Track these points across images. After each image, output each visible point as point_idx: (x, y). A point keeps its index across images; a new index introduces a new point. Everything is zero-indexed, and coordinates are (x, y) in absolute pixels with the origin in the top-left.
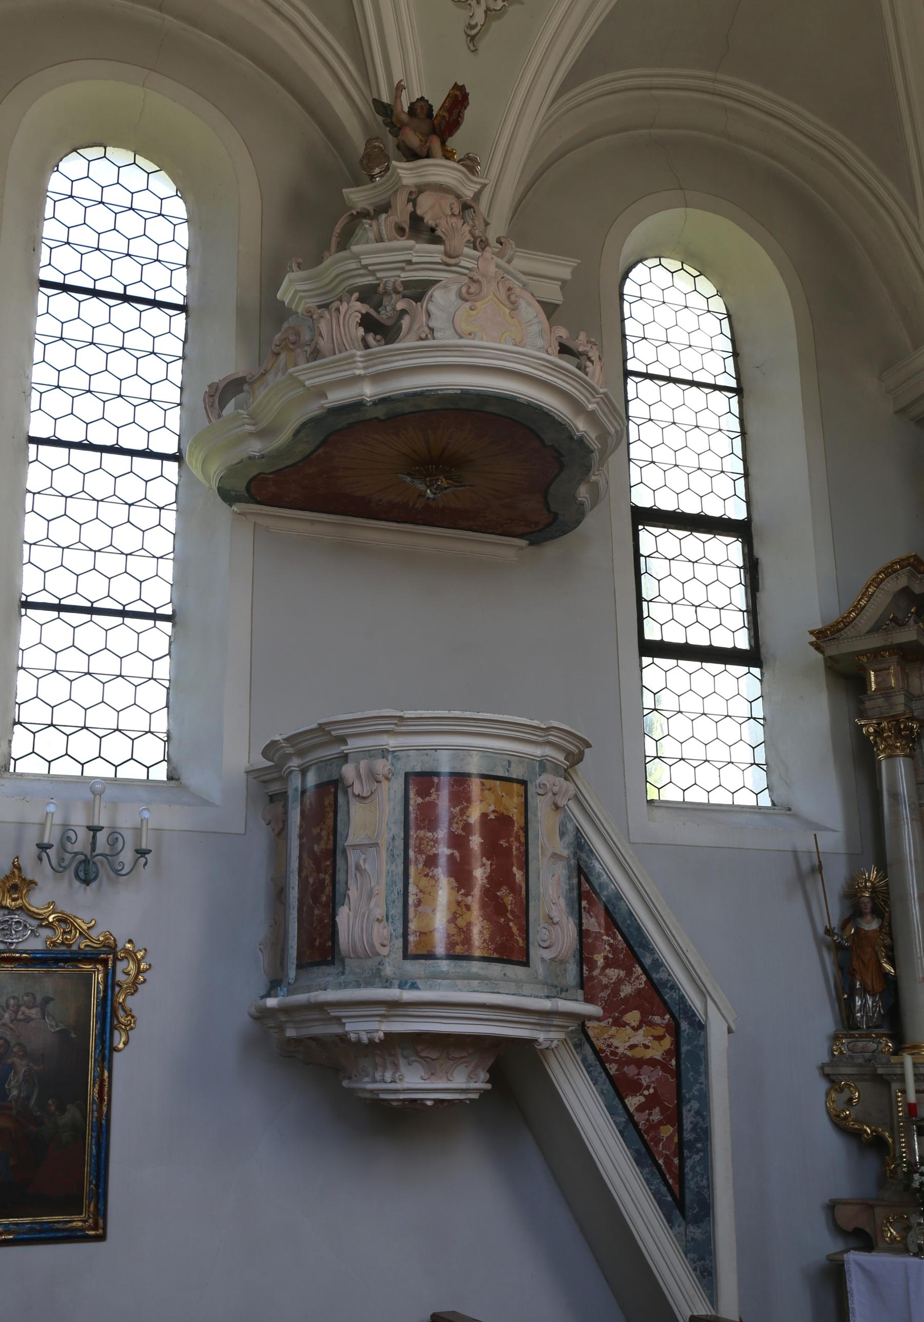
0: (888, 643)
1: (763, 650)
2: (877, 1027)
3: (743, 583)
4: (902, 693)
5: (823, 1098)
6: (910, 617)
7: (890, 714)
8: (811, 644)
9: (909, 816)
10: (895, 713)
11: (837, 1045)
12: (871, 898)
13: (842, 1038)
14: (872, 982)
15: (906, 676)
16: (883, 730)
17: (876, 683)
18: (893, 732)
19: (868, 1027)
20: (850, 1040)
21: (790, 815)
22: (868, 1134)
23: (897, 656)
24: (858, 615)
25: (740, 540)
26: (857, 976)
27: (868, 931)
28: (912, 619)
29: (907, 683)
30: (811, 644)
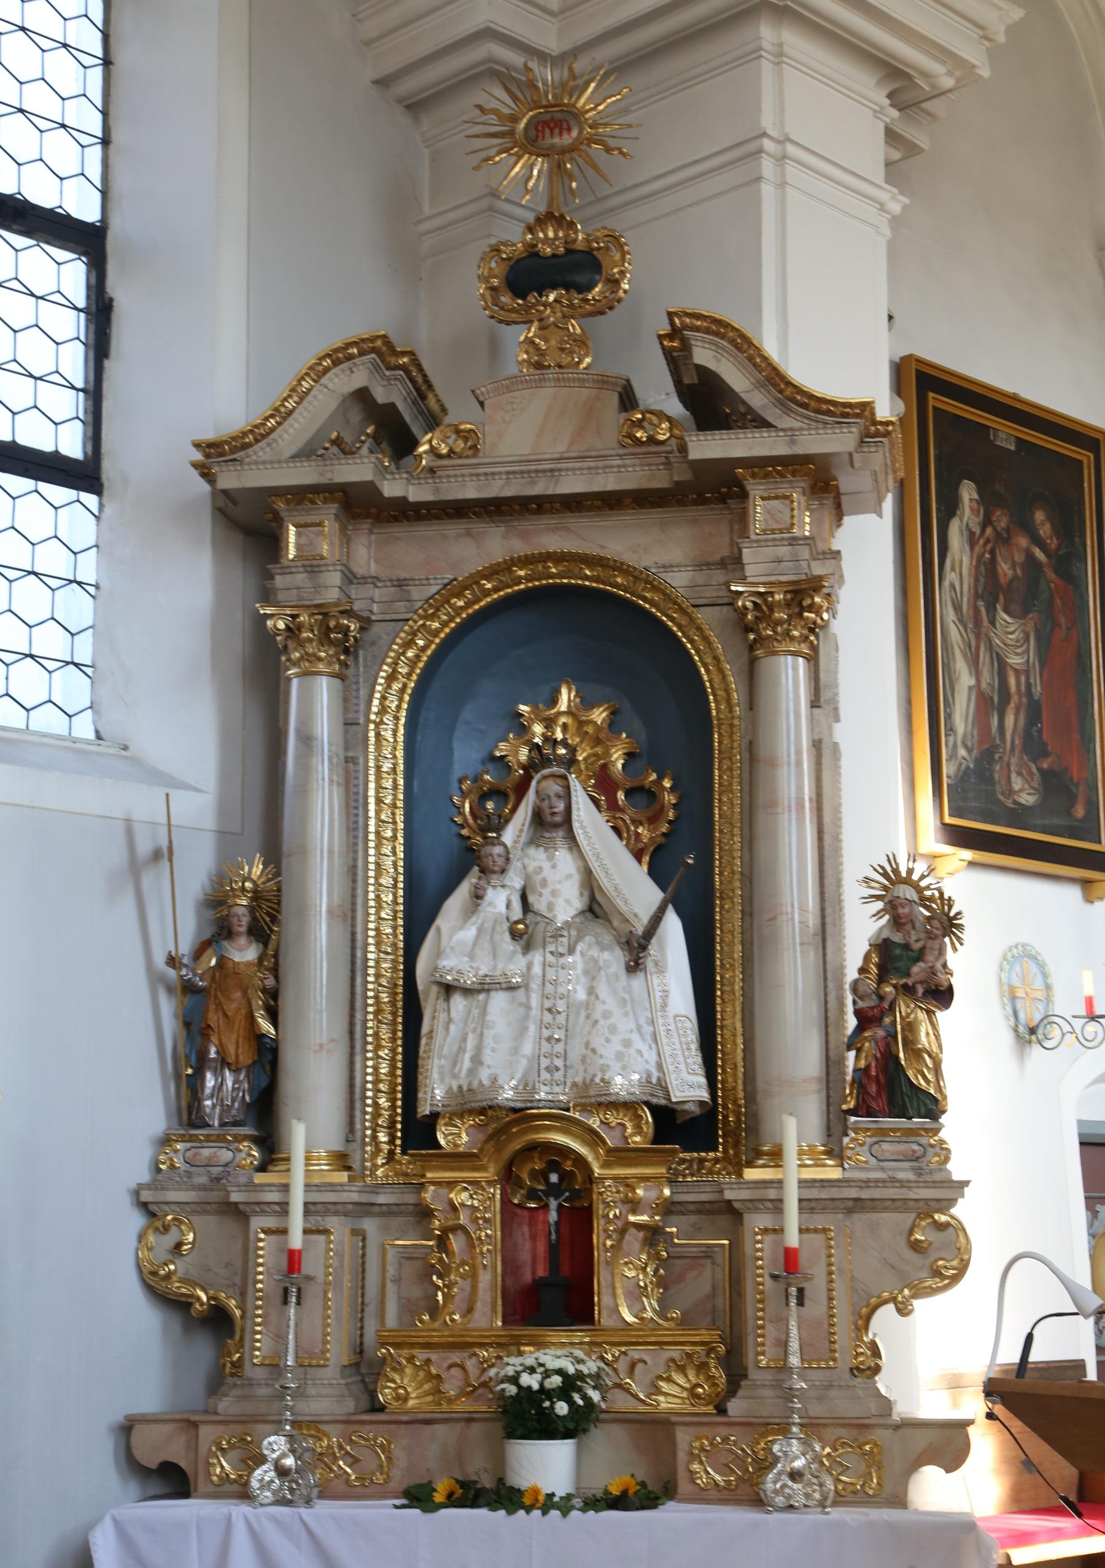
0: (324, 480)
2: (236, 1124)
3: (82, 338)
4: (339, 568)
5: (133, 1243)
6: (363, 442)
8: (195, 465)
9: (326, 777)
12: (252, 909)
13: (177, 1141)
15: (347, 540)
16: (300, 628)
17: (298, 546)
19: (223, 1124)
20: (189, 1145)
22: (202, 1304)
23: (336, 505)
24: (279, 424)
25: (84, 259)
27: (238, 963)
30: (195, 465)
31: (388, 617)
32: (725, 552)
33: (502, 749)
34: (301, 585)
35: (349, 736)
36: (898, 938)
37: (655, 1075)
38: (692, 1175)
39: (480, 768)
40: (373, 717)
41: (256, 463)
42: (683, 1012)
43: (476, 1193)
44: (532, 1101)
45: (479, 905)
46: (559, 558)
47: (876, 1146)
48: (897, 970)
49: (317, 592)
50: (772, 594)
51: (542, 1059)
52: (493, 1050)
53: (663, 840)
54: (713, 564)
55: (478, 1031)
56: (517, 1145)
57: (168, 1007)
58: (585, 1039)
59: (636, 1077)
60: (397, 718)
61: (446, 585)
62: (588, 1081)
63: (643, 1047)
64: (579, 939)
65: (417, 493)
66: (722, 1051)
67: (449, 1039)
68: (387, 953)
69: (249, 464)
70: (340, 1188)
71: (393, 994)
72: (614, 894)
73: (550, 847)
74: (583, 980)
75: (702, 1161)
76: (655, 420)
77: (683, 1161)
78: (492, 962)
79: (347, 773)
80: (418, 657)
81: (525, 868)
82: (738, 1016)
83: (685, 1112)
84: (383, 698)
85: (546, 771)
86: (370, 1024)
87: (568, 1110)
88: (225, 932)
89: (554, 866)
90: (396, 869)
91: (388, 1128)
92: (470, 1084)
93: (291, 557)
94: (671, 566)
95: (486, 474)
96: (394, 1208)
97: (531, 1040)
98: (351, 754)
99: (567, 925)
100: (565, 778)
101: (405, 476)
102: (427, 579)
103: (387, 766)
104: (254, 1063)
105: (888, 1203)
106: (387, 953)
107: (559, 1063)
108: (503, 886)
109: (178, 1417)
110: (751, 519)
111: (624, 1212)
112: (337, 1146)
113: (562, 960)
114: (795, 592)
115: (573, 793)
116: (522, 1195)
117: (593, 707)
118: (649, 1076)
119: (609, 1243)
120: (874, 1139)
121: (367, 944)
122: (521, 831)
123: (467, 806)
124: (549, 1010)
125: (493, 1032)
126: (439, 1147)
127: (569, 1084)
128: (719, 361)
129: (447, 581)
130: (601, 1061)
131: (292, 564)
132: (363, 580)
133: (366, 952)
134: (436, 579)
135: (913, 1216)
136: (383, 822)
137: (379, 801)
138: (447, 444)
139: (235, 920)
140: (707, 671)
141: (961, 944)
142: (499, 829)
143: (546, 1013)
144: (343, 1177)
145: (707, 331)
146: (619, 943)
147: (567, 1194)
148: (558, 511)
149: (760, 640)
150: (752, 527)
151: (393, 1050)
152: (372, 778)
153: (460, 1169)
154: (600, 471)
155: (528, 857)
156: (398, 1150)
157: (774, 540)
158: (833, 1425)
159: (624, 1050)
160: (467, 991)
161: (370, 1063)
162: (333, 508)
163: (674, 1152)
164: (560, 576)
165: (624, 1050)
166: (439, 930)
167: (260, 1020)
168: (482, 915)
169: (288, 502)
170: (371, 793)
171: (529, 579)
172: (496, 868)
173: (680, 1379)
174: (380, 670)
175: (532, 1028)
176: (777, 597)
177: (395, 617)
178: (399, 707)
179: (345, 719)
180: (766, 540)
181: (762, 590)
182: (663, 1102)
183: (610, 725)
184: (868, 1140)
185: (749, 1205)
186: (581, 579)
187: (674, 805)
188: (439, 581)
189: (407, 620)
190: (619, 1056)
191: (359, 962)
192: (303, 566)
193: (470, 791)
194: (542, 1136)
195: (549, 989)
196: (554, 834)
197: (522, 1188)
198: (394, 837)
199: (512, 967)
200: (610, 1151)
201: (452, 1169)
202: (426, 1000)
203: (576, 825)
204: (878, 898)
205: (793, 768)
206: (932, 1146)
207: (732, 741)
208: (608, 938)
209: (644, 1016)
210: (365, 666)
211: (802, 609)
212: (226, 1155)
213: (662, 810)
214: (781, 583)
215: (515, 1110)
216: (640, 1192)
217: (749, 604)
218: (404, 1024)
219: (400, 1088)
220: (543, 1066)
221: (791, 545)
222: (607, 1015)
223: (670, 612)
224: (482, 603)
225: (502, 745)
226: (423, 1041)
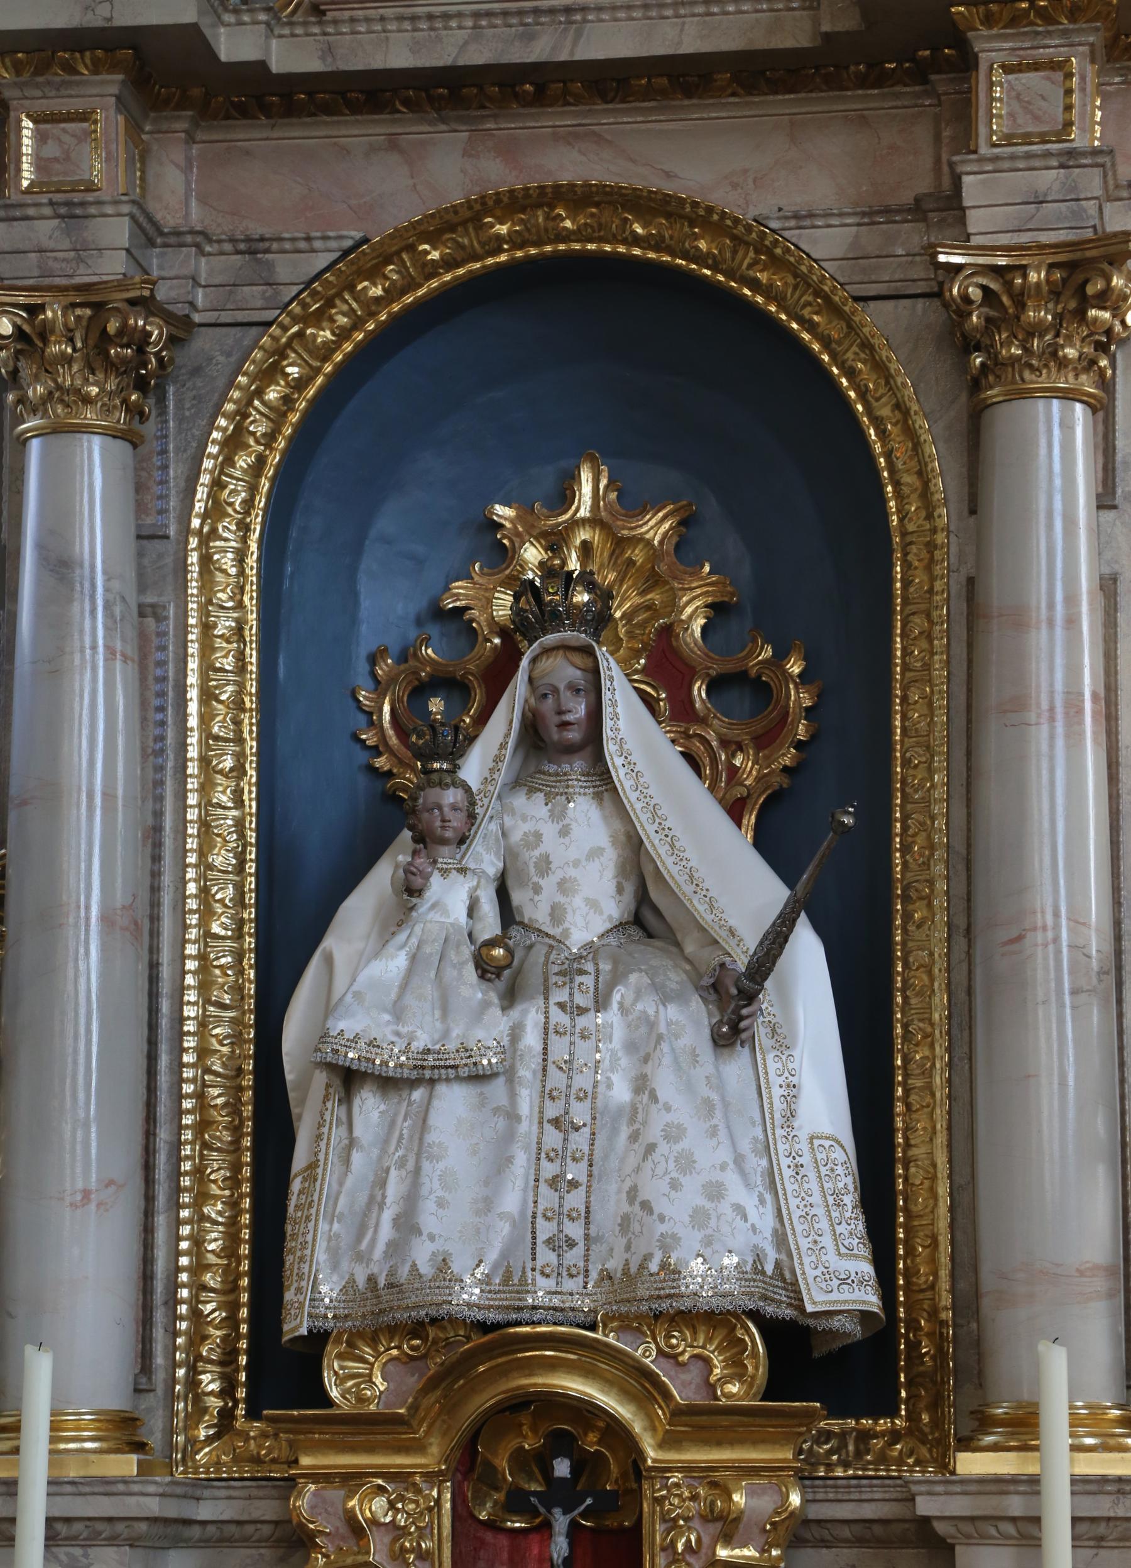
0: (95, 20)
4: (126, 209)
7: (77, 280)
9: (101, 642)
10: (95, 279)
15: (141, 156)
16: (45, 333)
17: (40, 164)
18: (79, 345)
23: (120, 77)
29: (142, 179)
31: (226, 317)
32: (923, 185)
33: (460, 593)
34: (51, 244)
35: (146, 561)
37: (771, 1256)
38: (846, 1465)
39: (413, 633)
40: (196, 523)
42: (828, 1130)
43: (402, 1498)
44: (519, 1309)
45: (412, 908)
49: (80, 260)
50: (1023, 270)
51: (540, 1220)
52: (441, 1204)
53: (785, 782)
54: (898, 212)
55: (411, 1165)
56: (486, 1399)
58: (628, 1184)
59: (733, 1260)
60: (244, 528)
61: (346, 253)
62: (633, 1269)
63: (750, 1203)
64: (617, 978)
66: (906, 1210)
67: (350, 1181)
70: (121, 1487)
72: (689, 889)
74: (624, 1062)
75: (864, 1436)
77: (827, 1435)
78: (438, 1024)
79: (143, 637)
80: (287, 400)
81: (504, 834)
82: (941, 1139)
83: (832, 1333)
84: (218, 484)
85: (551, 638)
86: (187, 1151)
87: (593, 1327)
89: (564, 832)
90: (242, 835)
91: (221, 1363)
92: (392, 1273)
93: (25, 183)
94: (811, 215)
96: (233, 1528)
97: (519, 1183)
98: (150, 599)
99: (591, 950)
100: (588, 651)
101: (262, 17)
102: (308, 239)
103: (224, 625)
107: (574, 1230)
108: (463, 871)
110: (982, 112)
111: (706, 1540)
112: (116, 1400)
113: (582, 1022)
114: (1071, 267)
115: (605, 684)
116: (496, 1503)
117: (644, 512)
118: (759, 1259)
121: (182, 989)
122: (498, 759)
123: (387, 708)
124: (556, 1122)
125: (441, 1166)
126: (328, 1402)
127: (594, 1275)
129: (348, 243)
130: (662, 1228)
131: (29, 199)
132: (176, 238)
133: (179, 1004)
134: (325, 238)
136: (217, 738)
137: (208, 696)
140: (882, 434)
142: (456, 752)
143: (549, 1128)
144: (128, 1464)
147: (589, 1501)
148: (578, 100)
149: (996, 366)
150: (982, 130)
151: (233, 1204)
152: (193, 648)
153: (370, 1449)
154: (669, 12)
155: (513, 812)
156: (241, 1411)
157: (1029, 156)
159: (708, 1205)
160: (388, 1084)
161: (185, 1230)
162: (112, 83)
163: (809, 1416)
164: (577, 235)
165: (708, 1205)
166: (329, 960)
168: (418, 929)
169: (18, 68)
170: (192, 679)
171: (517, 240)
172: (449, 834)
174: (211, 426)
175: (521, 1160)
176: (1033, 277)
177: (241, 316)
178: (249, 504)
179: (139, 527)
180: (1013, 157)
181: (1002, 261)
182: (788, 1313)
183: (678, 547)
185: (968, 1528)
186: (624, 242)
187: (807, 709)
188: (333, 244)
189: (269, 324)
190: (699, 1217)
191: (164, 1023)
193: (392, 680)
194: (539, 1380)
195: (556, 1078)
196: (566, 767)
197: (497, 1489)
198: (239, 770)
199: (480, 1034)
200: (679, 1413)
201: (353, 1449)
202: (302, 1102)
203: (610, 748)
205: (1059, 631)
207: (932, 579)
208: (675, 978)
209: (749, 1135)
210: (180, 420)
211: (1085, 302)
213: (783, 718)
214: (1042, 247)
215: (484, 1327)
216: (739, 1498)
217: (975, 293)
218: (256, 1149)
219: (245, 1282)
220: (541, 1237)
221: (1062, 166)
222: (673, 1134)
223: (806, 312)
224: (420, 292)
225: (460, 587)
226: (296, 1186)
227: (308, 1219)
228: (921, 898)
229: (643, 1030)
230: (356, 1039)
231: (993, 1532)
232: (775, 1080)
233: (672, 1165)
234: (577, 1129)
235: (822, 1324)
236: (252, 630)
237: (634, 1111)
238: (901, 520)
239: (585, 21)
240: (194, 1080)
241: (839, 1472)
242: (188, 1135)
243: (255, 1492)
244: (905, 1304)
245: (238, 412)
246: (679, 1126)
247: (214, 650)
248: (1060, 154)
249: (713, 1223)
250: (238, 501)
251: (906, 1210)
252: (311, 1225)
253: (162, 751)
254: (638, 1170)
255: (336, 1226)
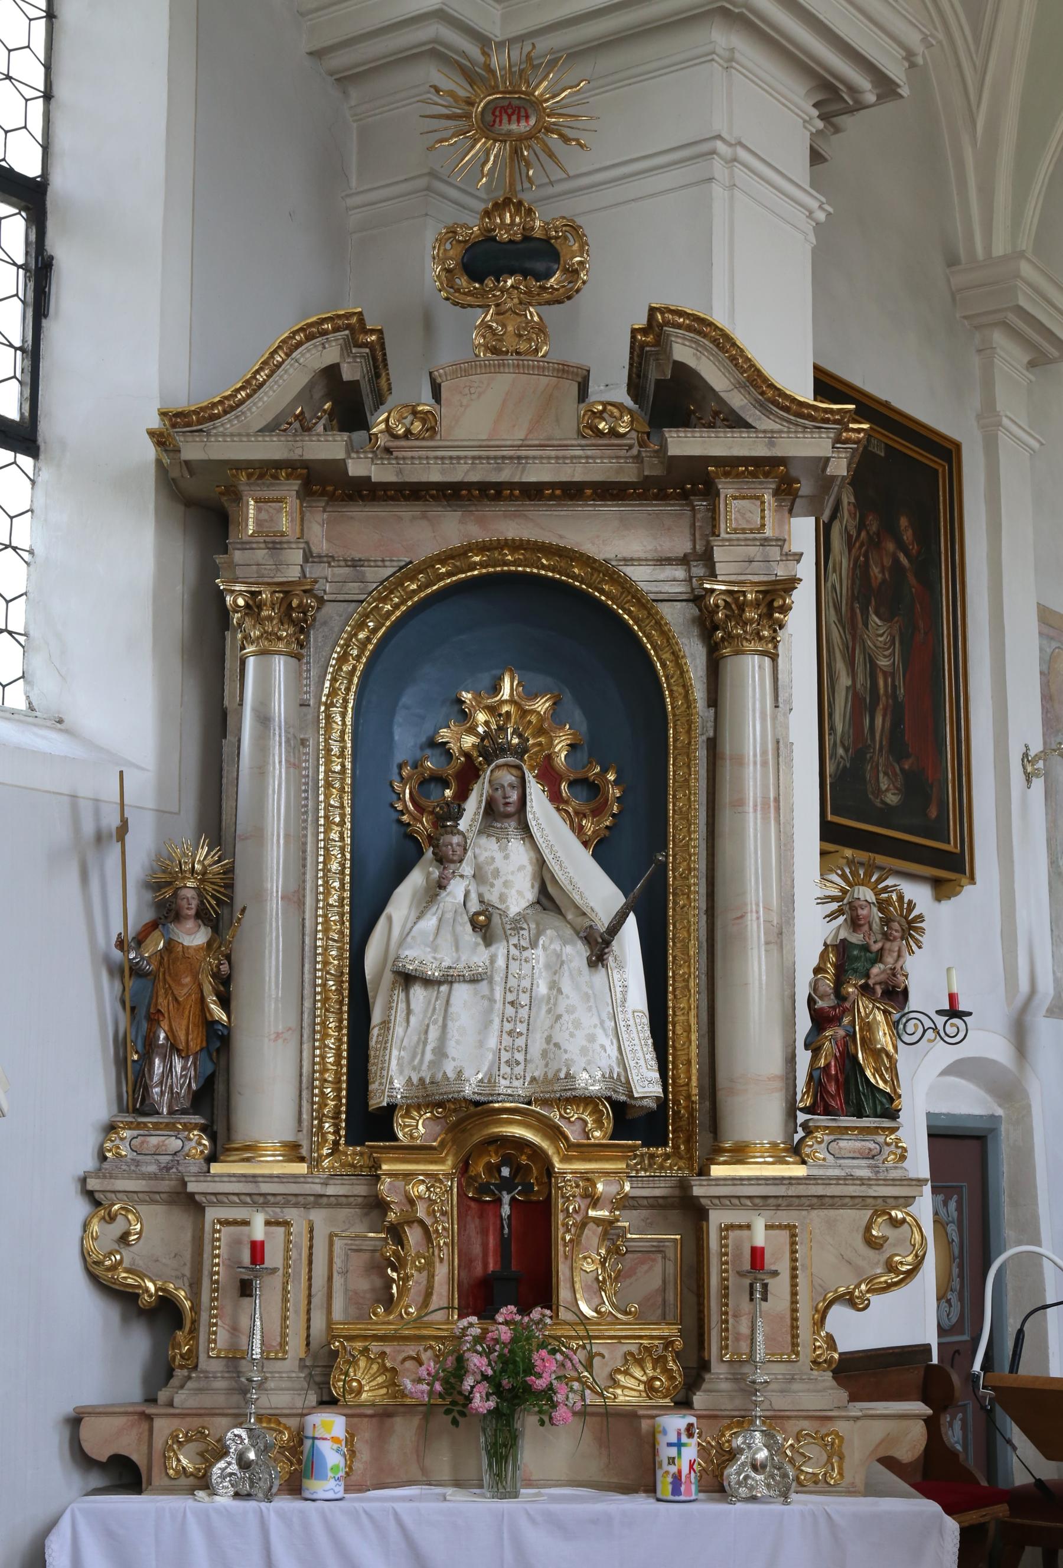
0: (295, 455)
1: (43, 426)
2: (184, 1112)
3: (21, 295)
5: (78, 1232)
6: (320, 418)
7: (276, 580)
8: (151, 433)
11: (112, 1141)
12: (200, 892)
13: (123, 1128)
14: (187, 1034)
16: (260, 606)
17: (258, 522)
19: (171, 1112)
20: (135, 1133)
21: (61, 730)
22: (150, 1296)
23: (299, 482)
24: (249, 396)
25: (23, 214)
26: (162, 1024)
27: (188, 948)
28: (323, 421)
30: (151, 433)
31: (340, 597)
34: (261, 561)
36: (856, 939)
37: (616, 1070)
38: (646, 1171)
40: (324, 699)
41: (224, 435)
43: (433, 1186)
44: (492, 1095)
46: (516, 546)
47: (834, 1144)
48: (855, 971)
49: (278, 570)
51: (503, 1051)
52: (458, 1042)
53: (607, 833)
56: (477, 1138)
57: (110, 990)
58: (546, 1034)
61: (401, 568)
63: (607, 1043)
64: (539, 933)
65: (380, 473)
66: (674, 1047)
67: (410, 1029)
68: (334, 941)
69: (216, 435)
70: (302, 1180)
71: (339, 983)
72: (570, 888)
73: (502, 838)
75: (652, 1156)
76: (616, 412)
78: (454, 954)
82: (693, 1013)
83: (642, 1107)
85: (501, 761)
86: (318, 1012)
87: (529, 1103)
88: (173, 914)
89: (506, 857)
90: (343, 855)
91: (333, 1118)
92: (433, 1077)
93: (251, 532)
94: (632, 559)
95: (451, 458)
96: (344, 1200)
99: (522, 917)
100: (519, 768)
101: (370, 455)
102: (383, 561)
104: (201, 1050)
105: (847, 1200)
106: (334, 941)
107: (520, 1057)
109: (131, 1409)
111: (583, 1207)
112: (289, 1137)
113: (526, 954)
115: (528, 784)
117: (536, 697)
118: (611, 1072)
119: (568, 1237)
120: (832, 1137)
123: (407, 791)
124: (512, 1003)
125: (457, 1024)
126: (396, 1139)
127: (528, 1079)
128: (698, 359)
129: (403, 563)
130: (566, 1056)
131: (254, 539)
132: (320, 559)
134: (391, 561)
135: (870, 1212)
136: (332, 806)
138: (404, 425)
139: (184, 903)
140: (663, 665)
141: (920, 947)
144: (302, 1168)
145: (689, 329)
146: (581, 938)
148: (517, 499)
149: (729, 637)
150: (722, 526)
151: (339, 1040)
153: (417, 1162)
154: (568, 461)
155: (480, 847)
156: (342, 1141)
157: (746, 539)
158: (796, 1417)
160: (428, 982)
161: (318, 1052)
162: (295, 485)
164: (515, 563)
166: (390, 919)
167: (212, 1006)
168: (441, 905)
169: (249, 476)
171: (482, 564)
172: (455, 858)
173: (637, 1372)
174: (333, 651)
176: (749, 596)
182: (623, 1098)
184: (826, 1138)
185: (716, 1201)
186: (537, 568)
188: (395, 564)
189: (362, 602)
190: (584, 1051)
192: (265, 542)
193: (410, 778)
194: (504, 1129)
195: (512, 982)
196: (506, 825)
198: (342, 823)
199: (476, 959)
200: (571, 1146)
203: (530, 816)
204: (833, 899)
206: (888, 1145)
208: (569, 932)
210: (316, 648)
212: (175, 1144)
214: (752, 583)
215: (477, 1104)
216: (600, 1187)
219: (344, 1078)
220: (503, 1060)
221: (762, 545)
222: (570, 1010)
223: (626, 606)
225: (444, 731)
226: (375, 1032)
227: (385, 1048)
228: (683, 894)
229: (554, 959)
230: (413, 961)
231: (728, 1203)
232: (618, 984)
233: (570, 1025)
234: (522, 1007)
235: (638, 1103)
236: (349, 751)
237: (549, 999)
238: (673, 708)
239: (527, 463)
240: (321, 978)
241: (643, 1173)
242: (319, 1005)
243: (355, 1182)
244: (672, 1093)
245: (344, 644)
246: (573, 1006)
247: (332, 762)
248: (761, 539)
249: (591, 1053)
250: (343, 687)
251: (674, 1047)
252: (388, 1052)
253: (306, 812)
254: (552, 1027)
255: (402, 1053)
